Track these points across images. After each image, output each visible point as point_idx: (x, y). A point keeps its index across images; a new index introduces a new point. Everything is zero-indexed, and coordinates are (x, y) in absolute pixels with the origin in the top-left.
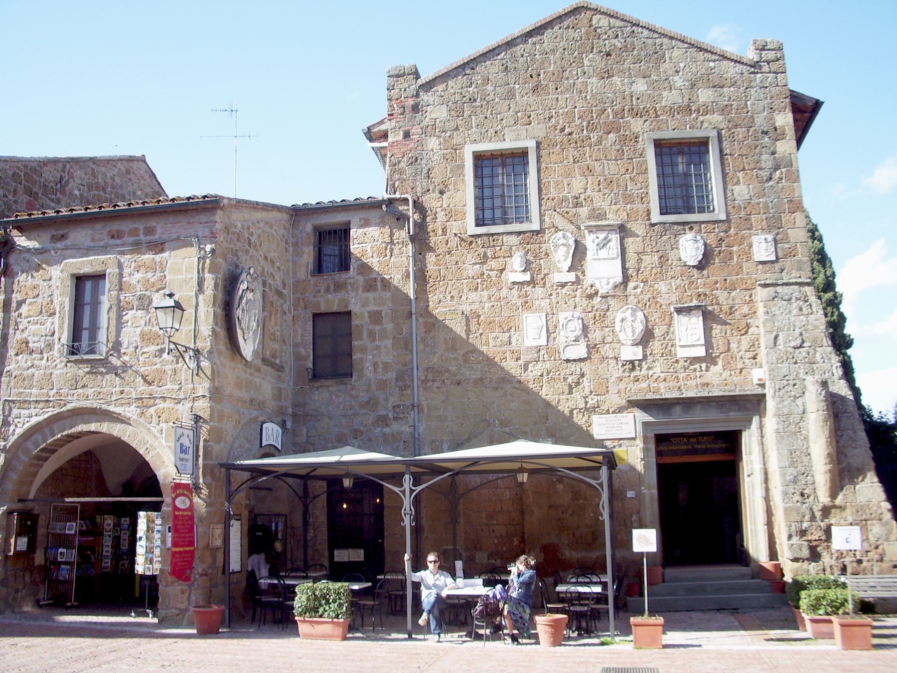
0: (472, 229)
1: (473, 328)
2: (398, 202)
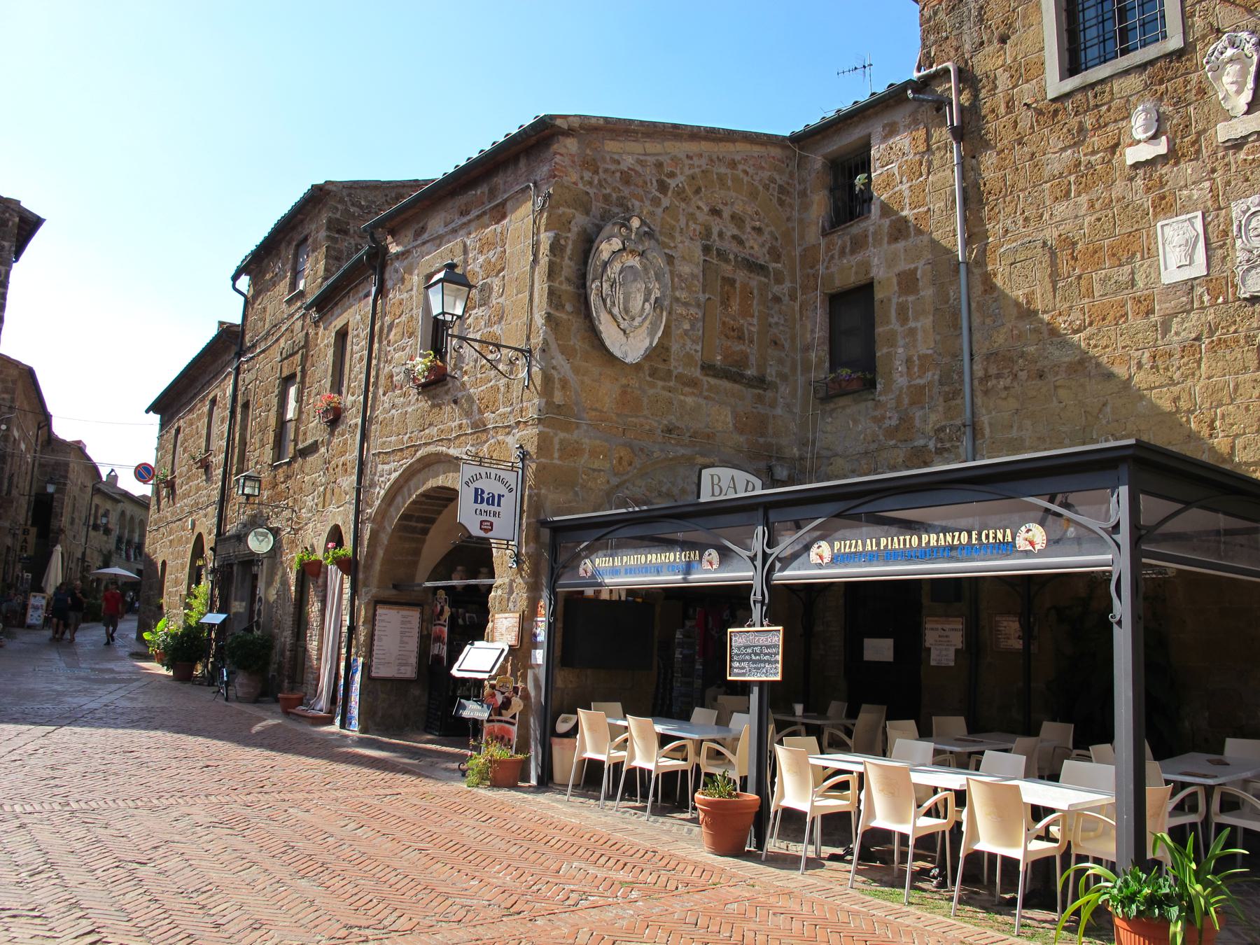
0: (1055, 84)
1: (1064, 269)
2: (938, 81)
